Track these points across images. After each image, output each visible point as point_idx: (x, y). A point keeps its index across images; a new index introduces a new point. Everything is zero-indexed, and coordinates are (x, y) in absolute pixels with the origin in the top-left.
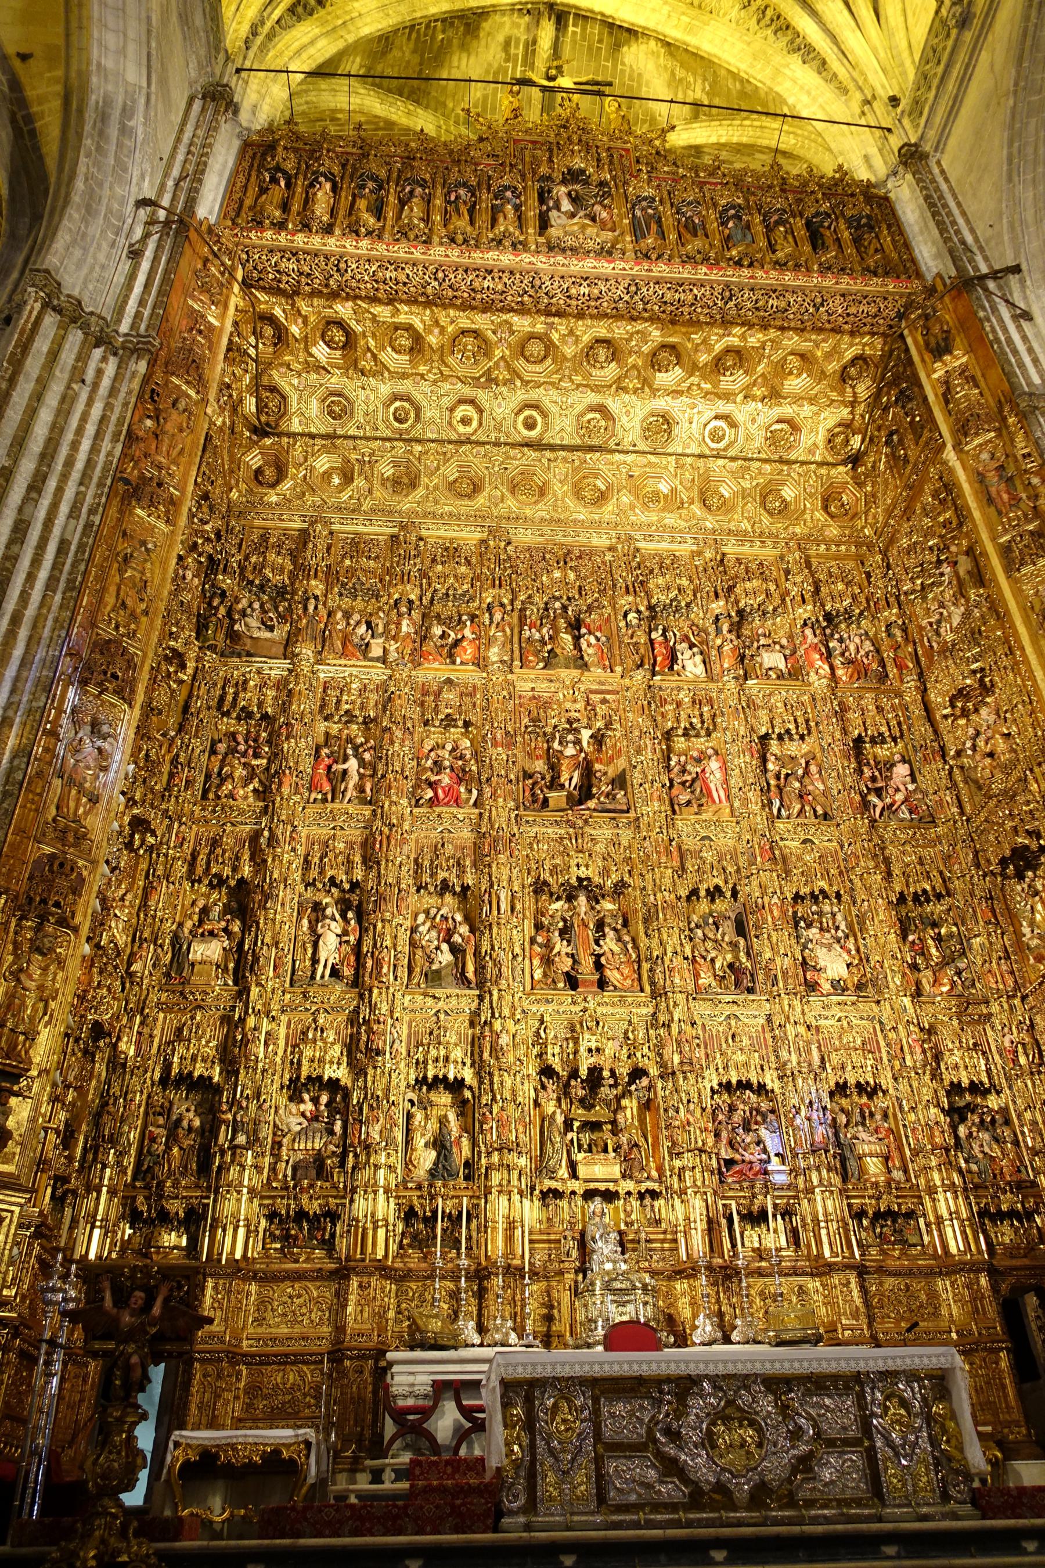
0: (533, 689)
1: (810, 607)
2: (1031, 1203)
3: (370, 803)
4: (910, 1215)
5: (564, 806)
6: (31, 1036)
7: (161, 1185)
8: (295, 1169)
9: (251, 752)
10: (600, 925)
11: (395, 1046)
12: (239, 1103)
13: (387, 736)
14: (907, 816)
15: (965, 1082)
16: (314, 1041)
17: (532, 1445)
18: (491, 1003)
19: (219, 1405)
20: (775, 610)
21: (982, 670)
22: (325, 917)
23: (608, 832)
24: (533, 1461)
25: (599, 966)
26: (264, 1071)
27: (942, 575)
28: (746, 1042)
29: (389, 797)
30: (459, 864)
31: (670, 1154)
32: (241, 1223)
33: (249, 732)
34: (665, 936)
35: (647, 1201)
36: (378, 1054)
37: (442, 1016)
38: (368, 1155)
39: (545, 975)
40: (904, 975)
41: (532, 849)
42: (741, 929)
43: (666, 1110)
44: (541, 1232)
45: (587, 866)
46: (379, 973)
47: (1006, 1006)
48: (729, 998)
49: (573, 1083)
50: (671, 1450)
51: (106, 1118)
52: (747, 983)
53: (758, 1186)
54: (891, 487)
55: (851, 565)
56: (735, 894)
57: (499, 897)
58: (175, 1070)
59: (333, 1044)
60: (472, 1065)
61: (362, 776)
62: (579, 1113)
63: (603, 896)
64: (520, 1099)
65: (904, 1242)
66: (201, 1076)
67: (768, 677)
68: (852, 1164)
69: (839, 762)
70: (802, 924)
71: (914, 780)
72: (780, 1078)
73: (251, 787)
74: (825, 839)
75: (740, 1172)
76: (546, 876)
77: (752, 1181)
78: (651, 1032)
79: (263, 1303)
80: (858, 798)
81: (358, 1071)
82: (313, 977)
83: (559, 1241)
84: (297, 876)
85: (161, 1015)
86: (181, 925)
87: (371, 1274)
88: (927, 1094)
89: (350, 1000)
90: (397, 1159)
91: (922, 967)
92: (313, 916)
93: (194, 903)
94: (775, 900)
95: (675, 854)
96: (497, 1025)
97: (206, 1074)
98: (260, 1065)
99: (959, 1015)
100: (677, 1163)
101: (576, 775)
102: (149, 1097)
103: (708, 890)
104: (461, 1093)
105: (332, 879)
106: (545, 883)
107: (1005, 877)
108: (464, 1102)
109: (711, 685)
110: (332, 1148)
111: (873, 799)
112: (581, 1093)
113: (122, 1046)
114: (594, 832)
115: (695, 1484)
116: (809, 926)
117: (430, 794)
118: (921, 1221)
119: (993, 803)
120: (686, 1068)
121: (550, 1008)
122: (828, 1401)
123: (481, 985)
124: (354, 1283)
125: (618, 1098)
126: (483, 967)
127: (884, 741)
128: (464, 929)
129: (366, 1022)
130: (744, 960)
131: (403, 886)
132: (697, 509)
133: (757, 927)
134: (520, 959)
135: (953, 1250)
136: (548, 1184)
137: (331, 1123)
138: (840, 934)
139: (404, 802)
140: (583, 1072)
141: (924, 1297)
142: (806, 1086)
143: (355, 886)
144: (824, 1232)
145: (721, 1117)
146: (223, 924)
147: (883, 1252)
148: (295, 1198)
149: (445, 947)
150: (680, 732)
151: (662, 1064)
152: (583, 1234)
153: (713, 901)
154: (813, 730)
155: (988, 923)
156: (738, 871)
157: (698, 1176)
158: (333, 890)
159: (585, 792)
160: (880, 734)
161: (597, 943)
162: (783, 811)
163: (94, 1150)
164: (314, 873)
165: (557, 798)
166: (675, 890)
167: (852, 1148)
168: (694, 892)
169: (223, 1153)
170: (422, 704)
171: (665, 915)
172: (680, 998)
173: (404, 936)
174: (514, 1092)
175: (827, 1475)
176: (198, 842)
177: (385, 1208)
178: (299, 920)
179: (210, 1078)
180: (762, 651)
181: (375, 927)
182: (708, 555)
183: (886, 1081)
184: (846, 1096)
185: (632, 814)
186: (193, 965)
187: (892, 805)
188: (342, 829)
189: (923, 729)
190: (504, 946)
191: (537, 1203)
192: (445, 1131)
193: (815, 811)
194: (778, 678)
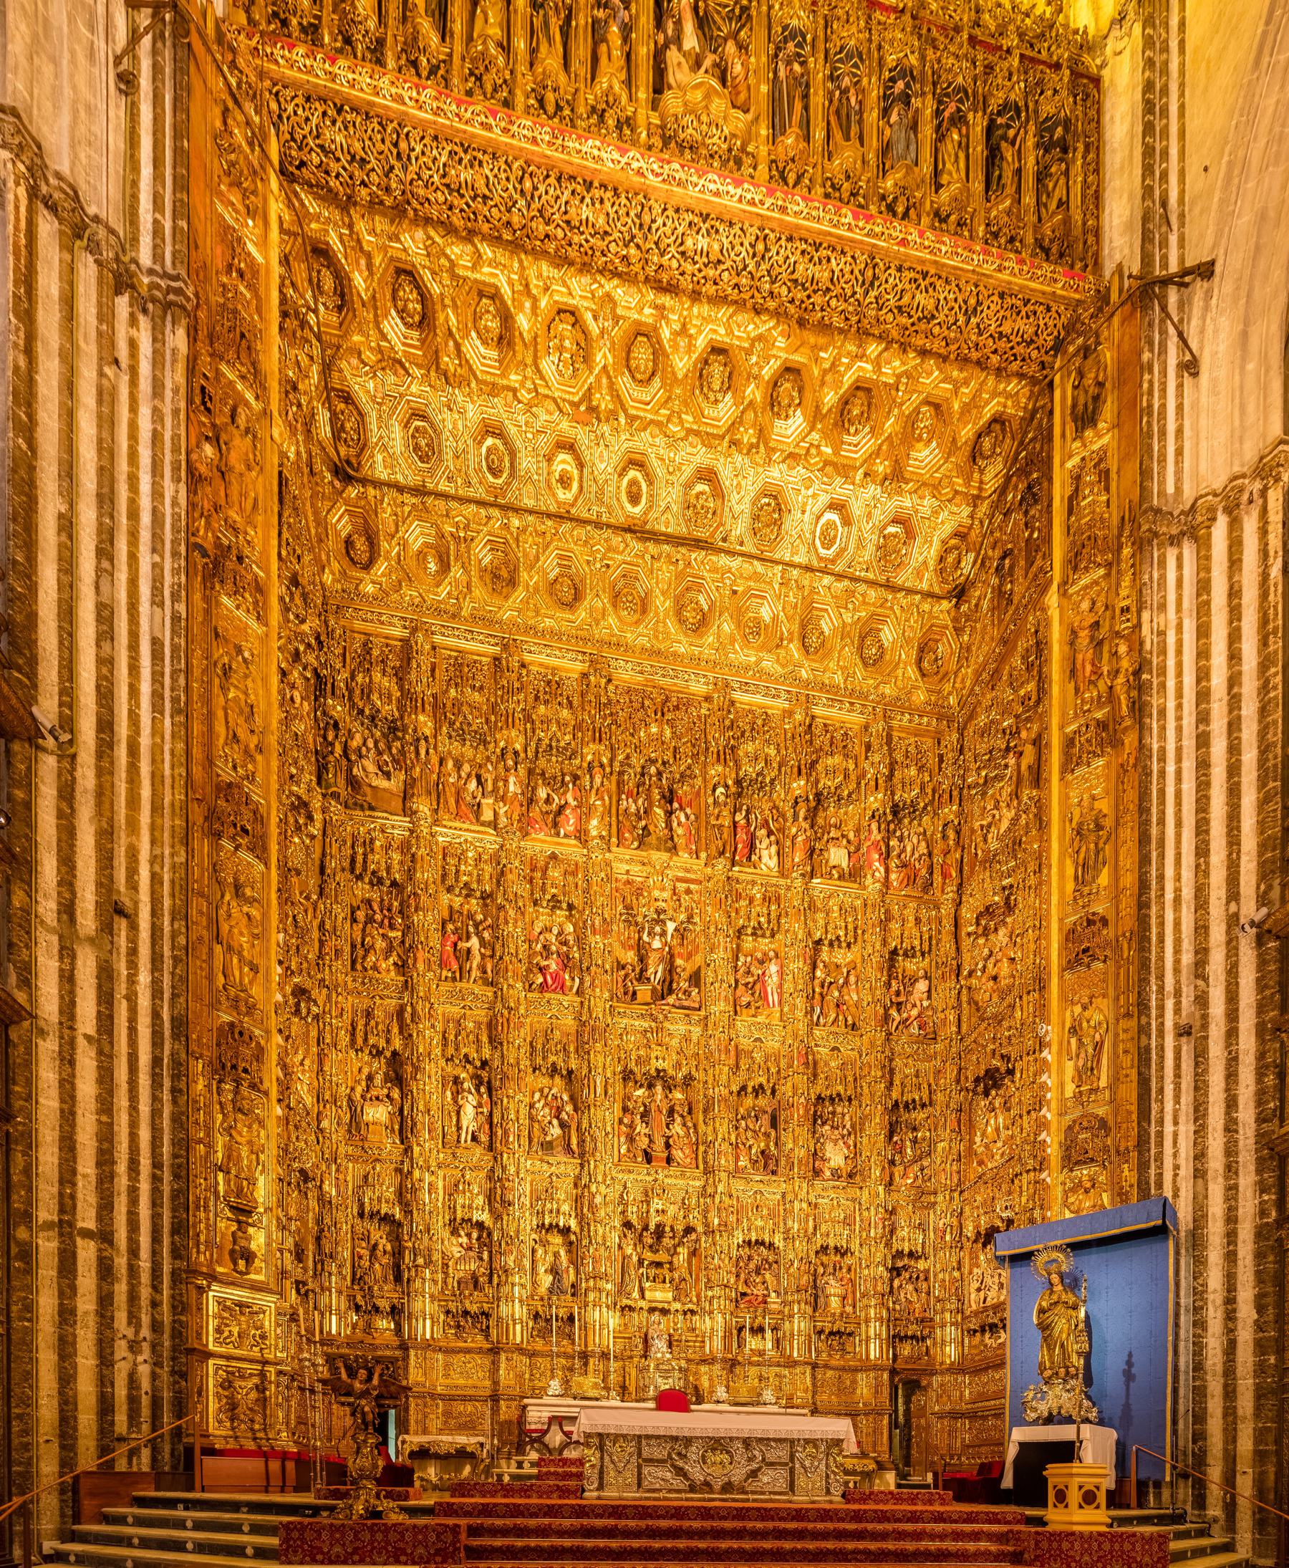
1: (880, 796)
15: (906, 1250)
20: (850, 795)
27: (1006, 766)
28: (765, 1212)
42: (774, 1123)
54: (987, 638)
55: (928, 743)
56: (773, 1092)
62: (649, 1256)
68: (821, 1300)
69: (874, 974)
76: (632, 1065)
80: (882, 1011)
90: (527, 1280)
100: (710, 1293)
101: (660, 968)
106: (631, 1072)
108: (571, 1243)
112: (650, 1241)
116: (824, 1123)
121: (632, 1176)
125: (675, 1247)
129: (500, 1180)
132: (794, 649)
136: (626, 1302)
139: (519, 985)
143: (484, 1064)
151: (707, 1225)
159: (667, 988)
165: (644, 991)
170: (531, 882)
172: (723, 1175)
173: (524, 1111)
178: (444, 1092)
180: (830, 845)
182: (798, 717)
183: (855, 1246)
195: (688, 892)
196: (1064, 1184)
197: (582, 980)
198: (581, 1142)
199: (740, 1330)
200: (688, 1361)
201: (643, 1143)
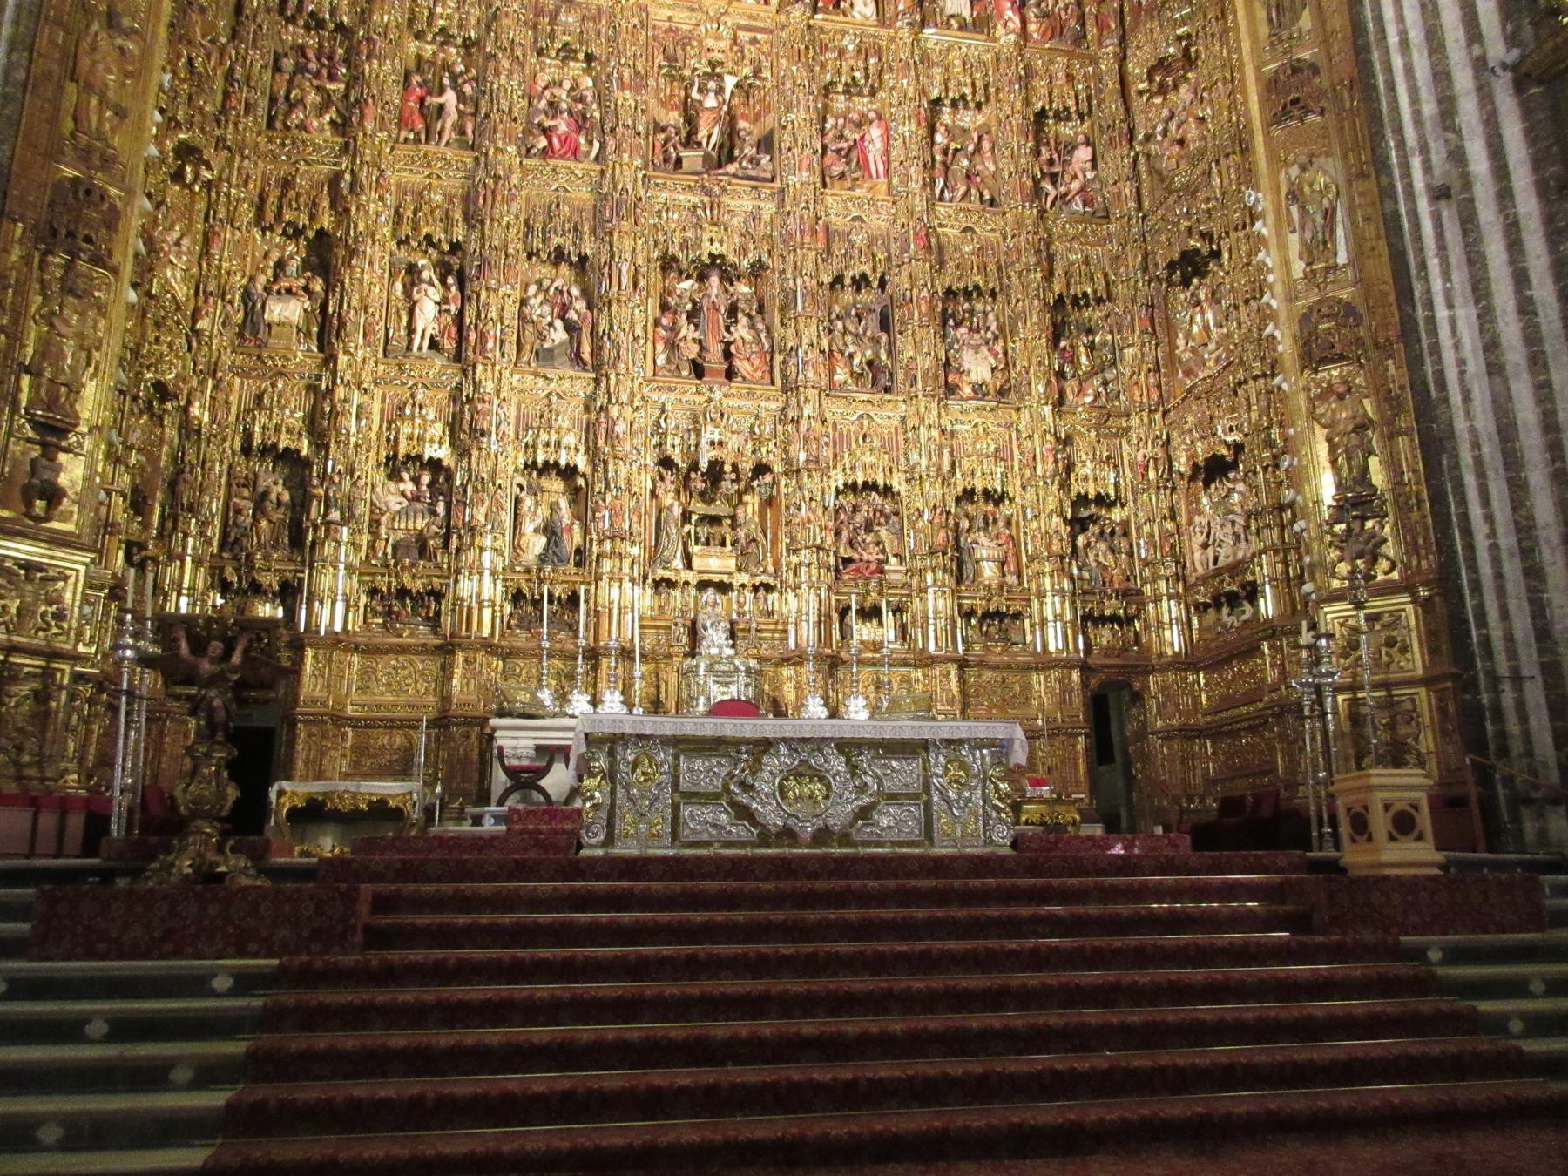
0: (670, 19)
2: (1133, 610)
3: (472, 148)
4: (1017, 616)
5: (699, 168)
6: (75, 389)
7: (250, 557)
8: (395, 547)
9: (324, 72)
10: (733, 311)
11: (502, 427)
12: (331, 478)
13: (491, 65)
14: (1080, 208)
15: (1092, 495)
16: (412, 417)
17: (613, 792)
18: (608, 388)
19: (325, 761)
21: (1189, 36)
22: (421, 281)
23: (748, 204)
24: (613, 805)
25: (728, 355)
26: (357, 446)
28: (876, 443)
29: (494, 142)
30: (576, 229)
31: (788, 550)
32: (340, 598)
33: (321, 46)
34: (801, 326)
35: (761, 593)
36: (482, 435)
37: (554, 399)
38: (473, 536)
39: (669, 361)
40: (1049, 382)
41: (660, 217)
42: (885, 324)
43: (787, 507)
44: (652, 618)
45: (721, 242)
46: (484, 347)
47: (1146, 420)
48: (865, 397)
49: (693, 475)
50: (744, 799)
51: (181, 487)
52: (884, 380)
53: (873, 583)
56: (882, 284)
57: (620, 271)
58: (257, 440)
59: (433, 422)
60: (586, 452)
61: (461, 114)
62: (699, 507)
63: (739, 279)
64: (635, 489)
65: (1007, 640)
66: (287, 449)
67: (949, 26)
70: (951, 322)
71: (1094, 167)
72: (908, 481)
73: (327, 118)
74: (988, 228)
75: (857, 570)
76: (675, 250)
77: (867, 579)
78: (779, 427)
79: (365, 673)
80: (1029, 183)
81: (462, 452)
82: (409, 348)
83: (669, 628)
84: (387, 231)
85: (238, 380)
86: (252, 279)
87: (477, 650)
88: (1052, 502)
89: (452, 376)
90: (504, 542)
91: (1069, 375)
92: (408, 279)
93: (266, 255)
94: (924, 293)
95: (821, 234)
96: (614, 411)
97: (293, 446)
98: (353, 440)
99: (1098, 427)
101: (716, 131)
102: (230, 467)
103: (853, 278)
104: (574, 480)
105: (428, 238)
106: (674, 259)
107: (1170, 283)
108: (577, 490)
109: (883, 31)
110: (434, 528)
111: (1047, 186)
112: (700, 486)
113: (195, 410)
114: (732, 203)
115: (763, 826)
116: (957, 325)
117: (542, 142)
118: (1027, 622)
119: (1174, 196)
120: (812, 466)
122: (894, 764)
123: (597, 368)
124: (460, 658)
125: (740, 494)
126: (601, 348)
127: (1068, 119)
128: (580, 305)
129: (470, 401)
130: (884, 357)
131: (511, 251)
133: (902, 323)
134: (642, 342)
135: (1052, 648)
136: (661, 573)
137: (433, 504)
138: (989, 335)
139: (512, 149)
140: (704, 465)
141: (1017, 689)
142: (933, 490)
143: (456, 247)
144: (931, 628)
145: (843, 517)
146: (302, 282)
147: (986, 648)
148: (396, 576)
149: (559, 324)
150: (840, 88)
151: (788, 462)
152: (694, 622)
153: (858, 290)
154: (992, 99)
155: (1144, 332)
156: (889, 259)
157: (814, 571)
158: (430, 250)
159: (726, 153)
160: (1066, 109)
161: (728, 329)
162: (946, 195)
163: (172, 521)
164: (406, 230)
166: (817, 276)
167: (971, 552)
168: (838, 280)
169: (316, 528)
171: (803, 302)
172: (812, 394)
173: (511, 309)
174: (629, 481)
175: (884, 822)
176: (266, 181)
177: (491, 589)
178: (391, 283)
179: (298, 451)
181: (478, 296)
183: (1014, 489)
184: (973, 502)
185: (777, 185)
186: (269, 325)
187: (1066, 194)
188: (439, 177)
189: (1114, 106)
190: (625, 326)
191: (649, 591)
192: (555, 517)
193: (981, 195)
194: (960, 28)
195: (754, 41)
196: (1307, 389)
197: (603, 145)
198: (597, 351)
199: (844, 612)
200: (761, 659)
201: (692, 351)
